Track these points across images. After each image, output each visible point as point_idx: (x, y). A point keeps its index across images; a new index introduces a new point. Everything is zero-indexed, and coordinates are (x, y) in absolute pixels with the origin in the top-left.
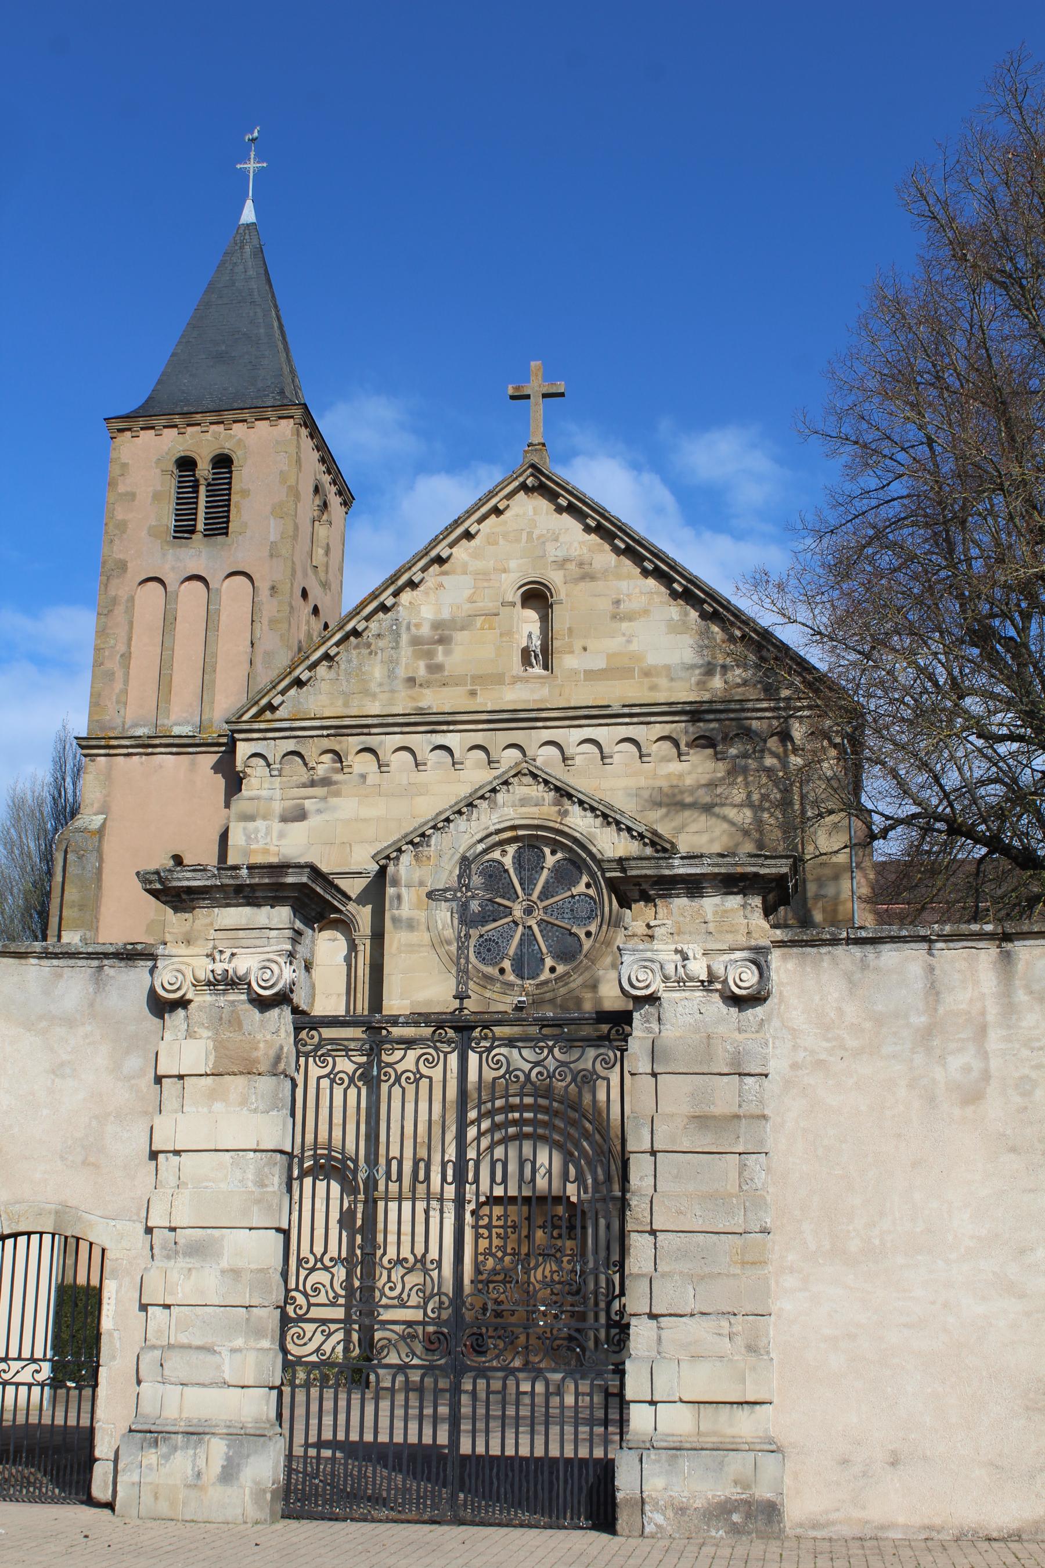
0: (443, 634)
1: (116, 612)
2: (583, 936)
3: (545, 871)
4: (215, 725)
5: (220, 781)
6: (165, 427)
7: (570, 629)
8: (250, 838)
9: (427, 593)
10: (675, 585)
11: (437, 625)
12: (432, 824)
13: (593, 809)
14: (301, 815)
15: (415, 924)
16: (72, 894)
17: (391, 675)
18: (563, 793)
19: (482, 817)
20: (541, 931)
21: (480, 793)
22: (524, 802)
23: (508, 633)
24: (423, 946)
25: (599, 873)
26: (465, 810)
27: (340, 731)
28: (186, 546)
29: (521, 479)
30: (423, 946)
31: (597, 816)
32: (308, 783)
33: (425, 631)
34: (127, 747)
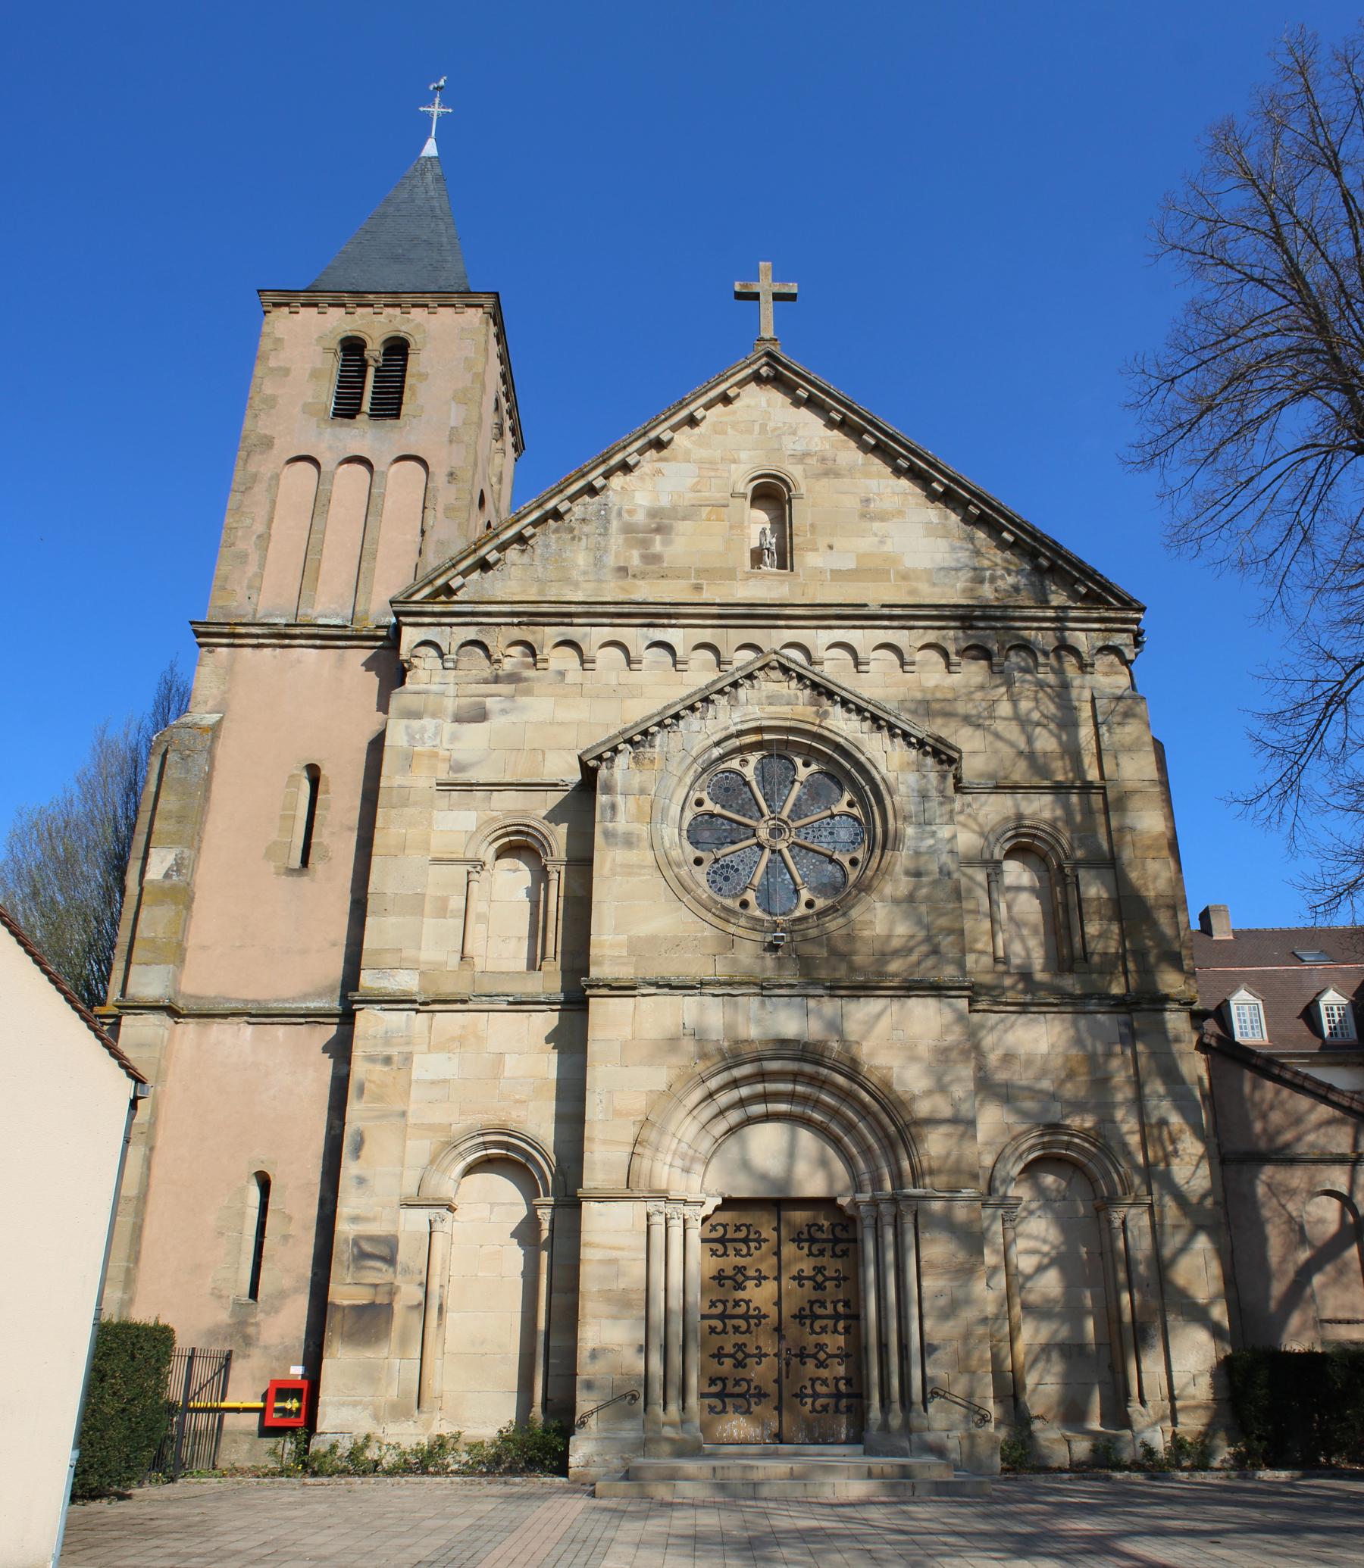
0: (661, 523)
1: (256, 489)
2: (847, 864)
3: (797, 785)
4: (371, 618)
5: (373, 680)
6: (331, 305)
7: (812, 525)
8: (413, 738)
9: (641, 478)
10: (935, 485)
11: (653, 513)
12: (657, 719)
13: (860, 710)
14: (480, 715)
15: (634, 840)
16: (168, 802)
17: (598, 563)
18: (823, 691)
19: (720, 715)
20: (793, 857)
21: (719, 686)
22: (772, 700)
23: (738, 526)
24: (645, 867)
25: (867, 788)
26: (699, 705)
27: (534, 618)
28: (348, 425)
29: (755, 367)
30: (645, 867)
31: (864, 719)
32: (491, 679)
33: (640, 517)
34: (257, 636)
